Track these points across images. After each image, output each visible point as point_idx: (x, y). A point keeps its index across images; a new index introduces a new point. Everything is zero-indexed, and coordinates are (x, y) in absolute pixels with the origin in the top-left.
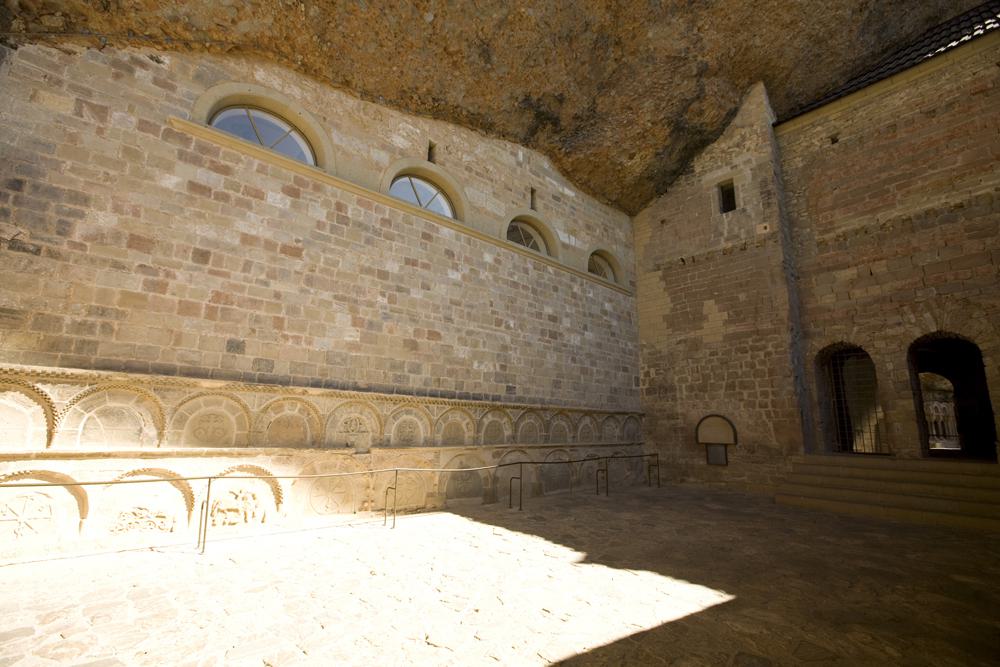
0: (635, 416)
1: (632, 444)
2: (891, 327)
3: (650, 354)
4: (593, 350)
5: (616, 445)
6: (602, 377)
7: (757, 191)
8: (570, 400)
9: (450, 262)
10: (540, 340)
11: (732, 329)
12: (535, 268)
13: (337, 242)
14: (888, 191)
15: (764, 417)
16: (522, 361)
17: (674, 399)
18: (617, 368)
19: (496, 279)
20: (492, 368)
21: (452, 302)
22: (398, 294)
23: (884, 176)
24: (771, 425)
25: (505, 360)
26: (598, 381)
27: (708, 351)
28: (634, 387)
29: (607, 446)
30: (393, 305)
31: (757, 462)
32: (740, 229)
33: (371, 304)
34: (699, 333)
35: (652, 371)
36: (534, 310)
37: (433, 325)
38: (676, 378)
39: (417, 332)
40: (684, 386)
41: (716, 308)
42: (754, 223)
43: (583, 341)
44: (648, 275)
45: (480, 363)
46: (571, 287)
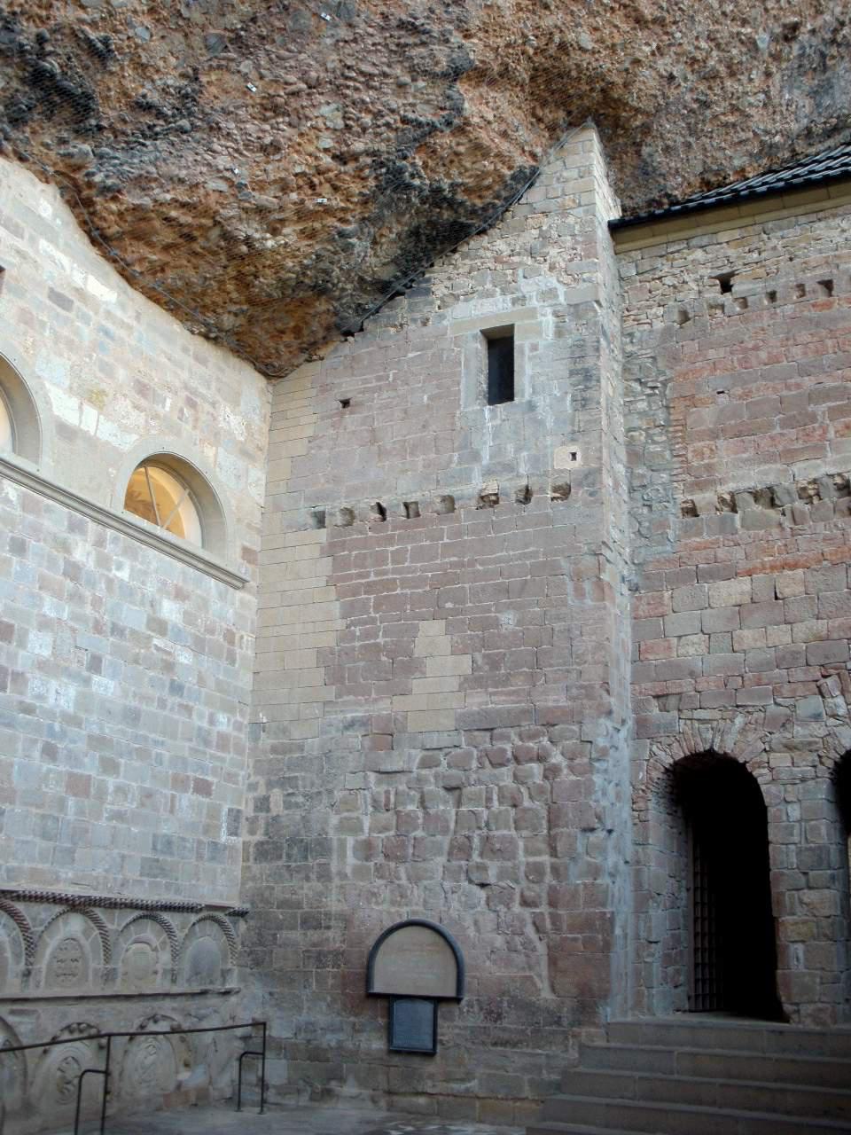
0: (220, 915)
1: (203, 993)
2: (804, 722)
3: (274, 750)
4: (111, 729)
5: (155, 996)
6: (130, 806)
7: (562, 368)
8: (26, 865)
11: (477, 701)
14: (813, 418)
15: (530, 930)
17: (324, 875)
18: (179, 783)
23: (808, 382)
24: (541, 948)
26: (119, 816)
27: (418, 755)
28: (224, 838)
29: (128, 997)
31: (505, 1043)
32: (518, 450)
34: (400, 704)
35: (277, 796)
38: (334, 820)
41: (445, 642)
42: (549, 441)
43: (84, 701)
44: (292, 538)
46: (65, 547)
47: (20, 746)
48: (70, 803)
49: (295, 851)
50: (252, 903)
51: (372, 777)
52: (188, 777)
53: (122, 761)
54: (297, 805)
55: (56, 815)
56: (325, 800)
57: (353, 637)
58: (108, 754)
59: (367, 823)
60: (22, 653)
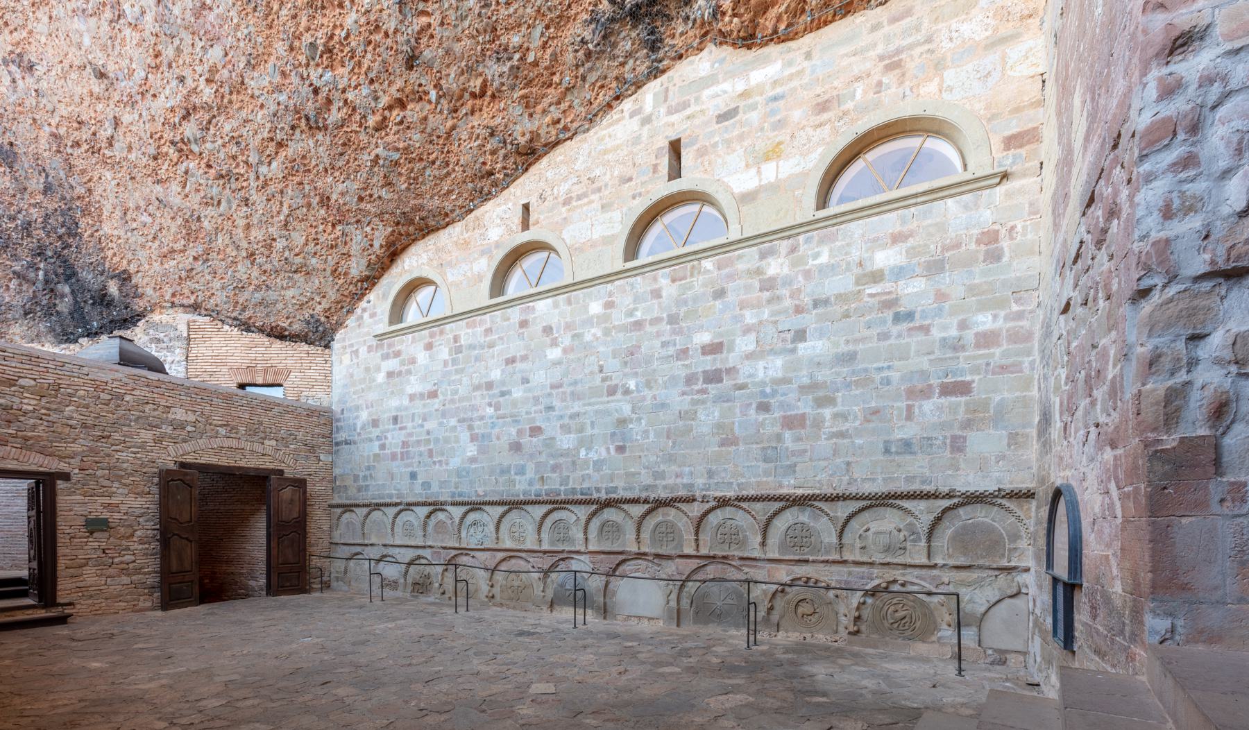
9: (548, 340)
10: (684, 393)
12: (673, 281)
13: (457, 372)
16: (652, 435)
19: (607, 332)
20: (604, 454)
21: (553, 387)
22: (501, 399)
25: (624, 440)
30: (499, 412)
33: (482, 418)
36: (671, 350)
37: (533, 420)
39: (520, 432)
45: (589, 449)
47: (738, 411)
48: (787, 436)
52: (930, 386)
53: (840, 394)
55: (774, 445)
58: (821, 394)
60: (732, 355)
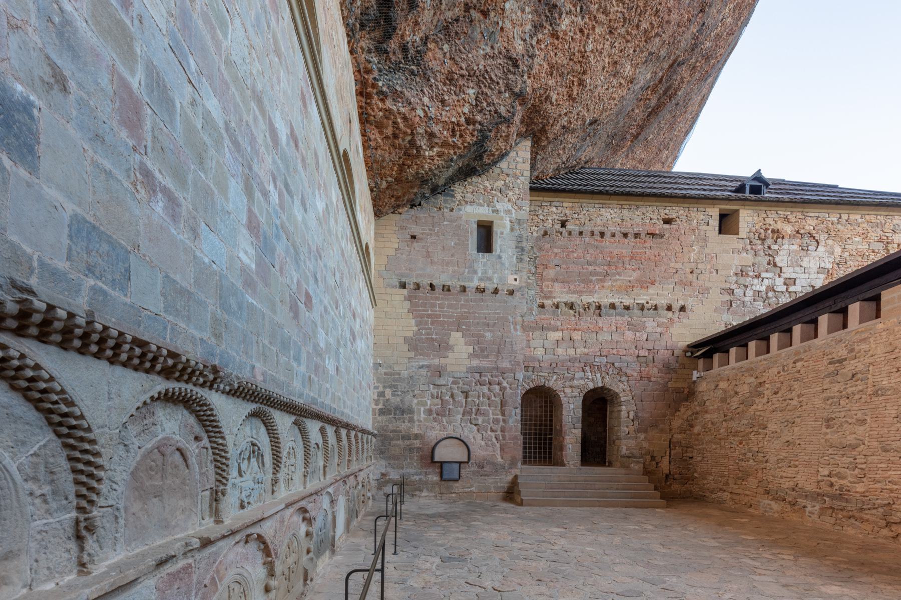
2: (577, 380)
3: (386, 374)
11: (475, 362)
14: (591, 281)
17: (411, 420)
23: (591, 268)
27: (451, 379)
32: (494, 273)
34: (443, 361)
35: (388, 392)
40: (422, 409)
41: (462, 341)
42: (506, 272)
44: (389, 290)
49: (398, 412)
50: (378, 431)
51: (431, 386)
54: (398, 395)
56: (411, 394)
57: (421, 334)
59: (429, 402)
